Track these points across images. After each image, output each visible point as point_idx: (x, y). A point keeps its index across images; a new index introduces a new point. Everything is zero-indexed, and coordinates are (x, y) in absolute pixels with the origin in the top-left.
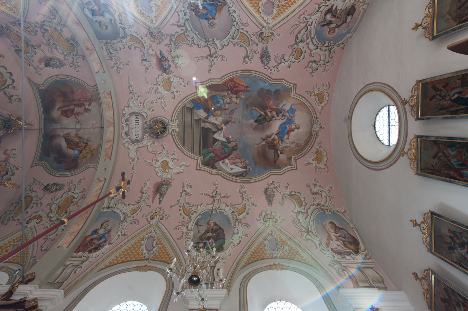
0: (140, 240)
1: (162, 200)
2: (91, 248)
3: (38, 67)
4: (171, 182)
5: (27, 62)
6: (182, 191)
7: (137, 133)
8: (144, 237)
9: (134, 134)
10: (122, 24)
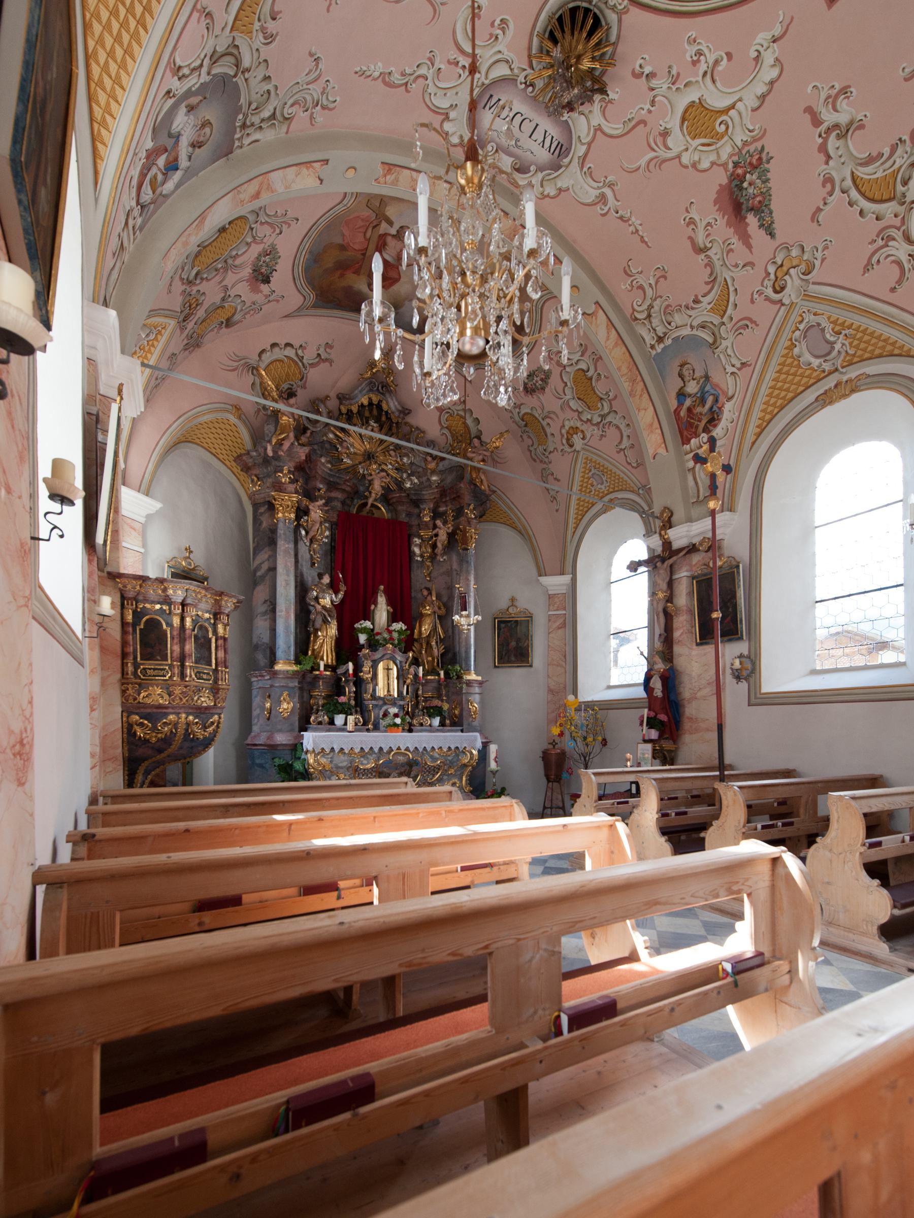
0: (787, 351)
1: (772, 222)
2: (702, 425)
3: (267, 296)
4: (763, 148)
5: (252, 312)
6: (820, 140)
7: (539, 135)
8: (791, 339)
9: (535, 147)
10: (201, 65)
